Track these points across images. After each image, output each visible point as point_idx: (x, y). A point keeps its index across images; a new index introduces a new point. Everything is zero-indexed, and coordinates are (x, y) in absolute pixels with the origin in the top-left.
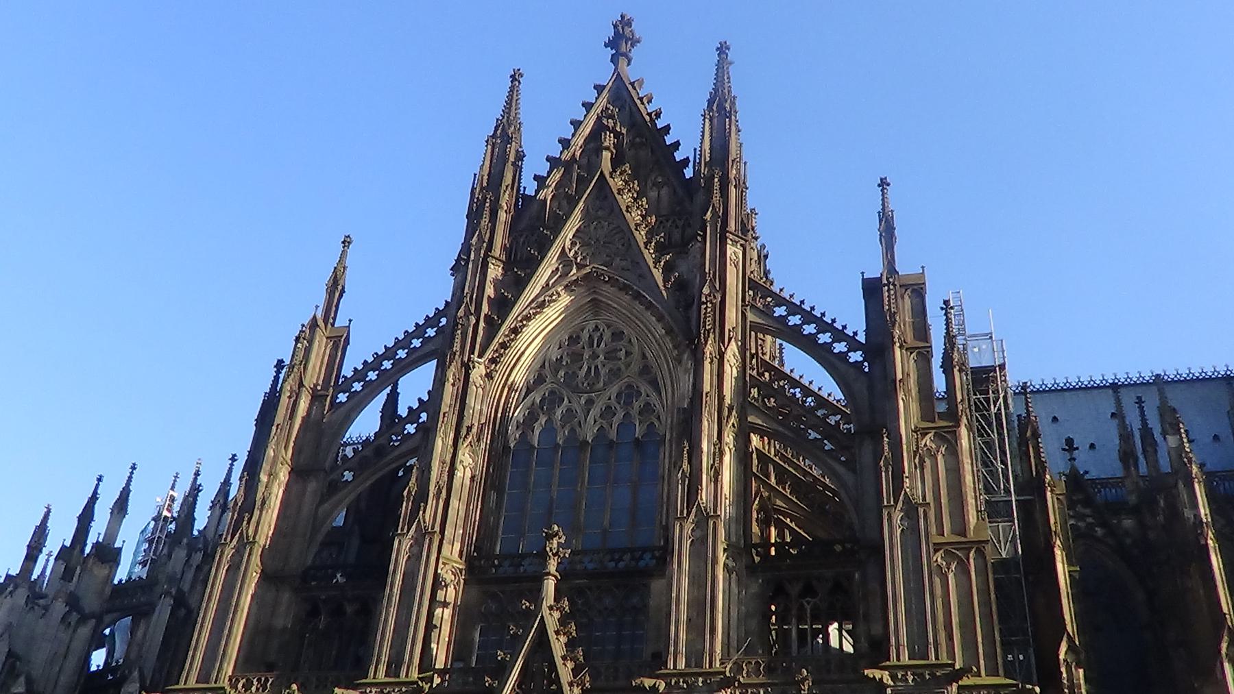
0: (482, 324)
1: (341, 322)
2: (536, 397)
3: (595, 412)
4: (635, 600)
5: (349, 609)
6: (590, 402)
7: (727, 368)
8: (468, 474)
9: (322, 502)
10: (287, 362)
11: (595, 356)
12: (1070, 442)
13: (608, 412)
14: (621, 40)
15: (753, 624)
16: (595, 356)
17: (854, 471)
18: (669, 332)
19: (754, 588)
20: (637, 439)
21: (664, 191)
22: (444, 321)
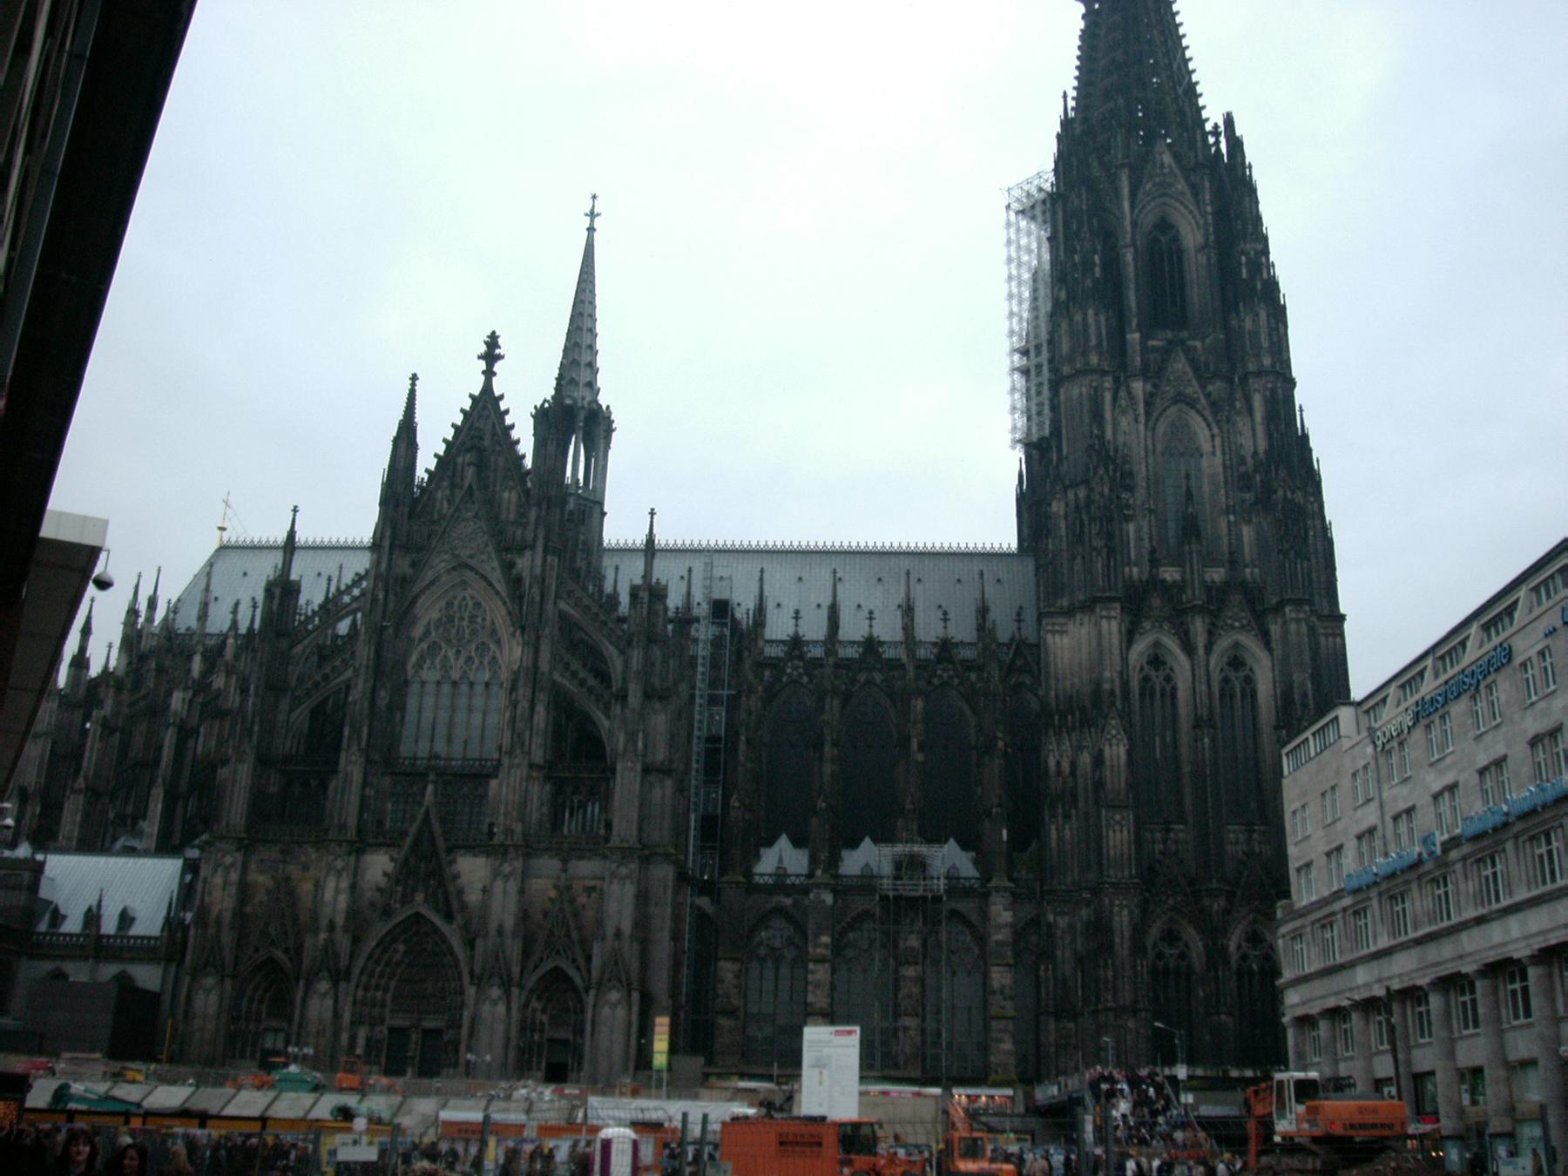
0: (391, 596)
1: (294, 576)
2: (424, 646)
4: (480, 791)
5: (313, 783)
6: (458, 652)
9: (291, 711)
10: (260, 604)
11: (462, 619)
12: (797, 612)
13: (469, 659)
14: (491, 355)
15: (545, 810)
16: (462, 619)
17: (608, 717)
18: (510, 613)
19: (548, 788)
20: (487, 685)
21: (514, 495)
22: (364, 584)
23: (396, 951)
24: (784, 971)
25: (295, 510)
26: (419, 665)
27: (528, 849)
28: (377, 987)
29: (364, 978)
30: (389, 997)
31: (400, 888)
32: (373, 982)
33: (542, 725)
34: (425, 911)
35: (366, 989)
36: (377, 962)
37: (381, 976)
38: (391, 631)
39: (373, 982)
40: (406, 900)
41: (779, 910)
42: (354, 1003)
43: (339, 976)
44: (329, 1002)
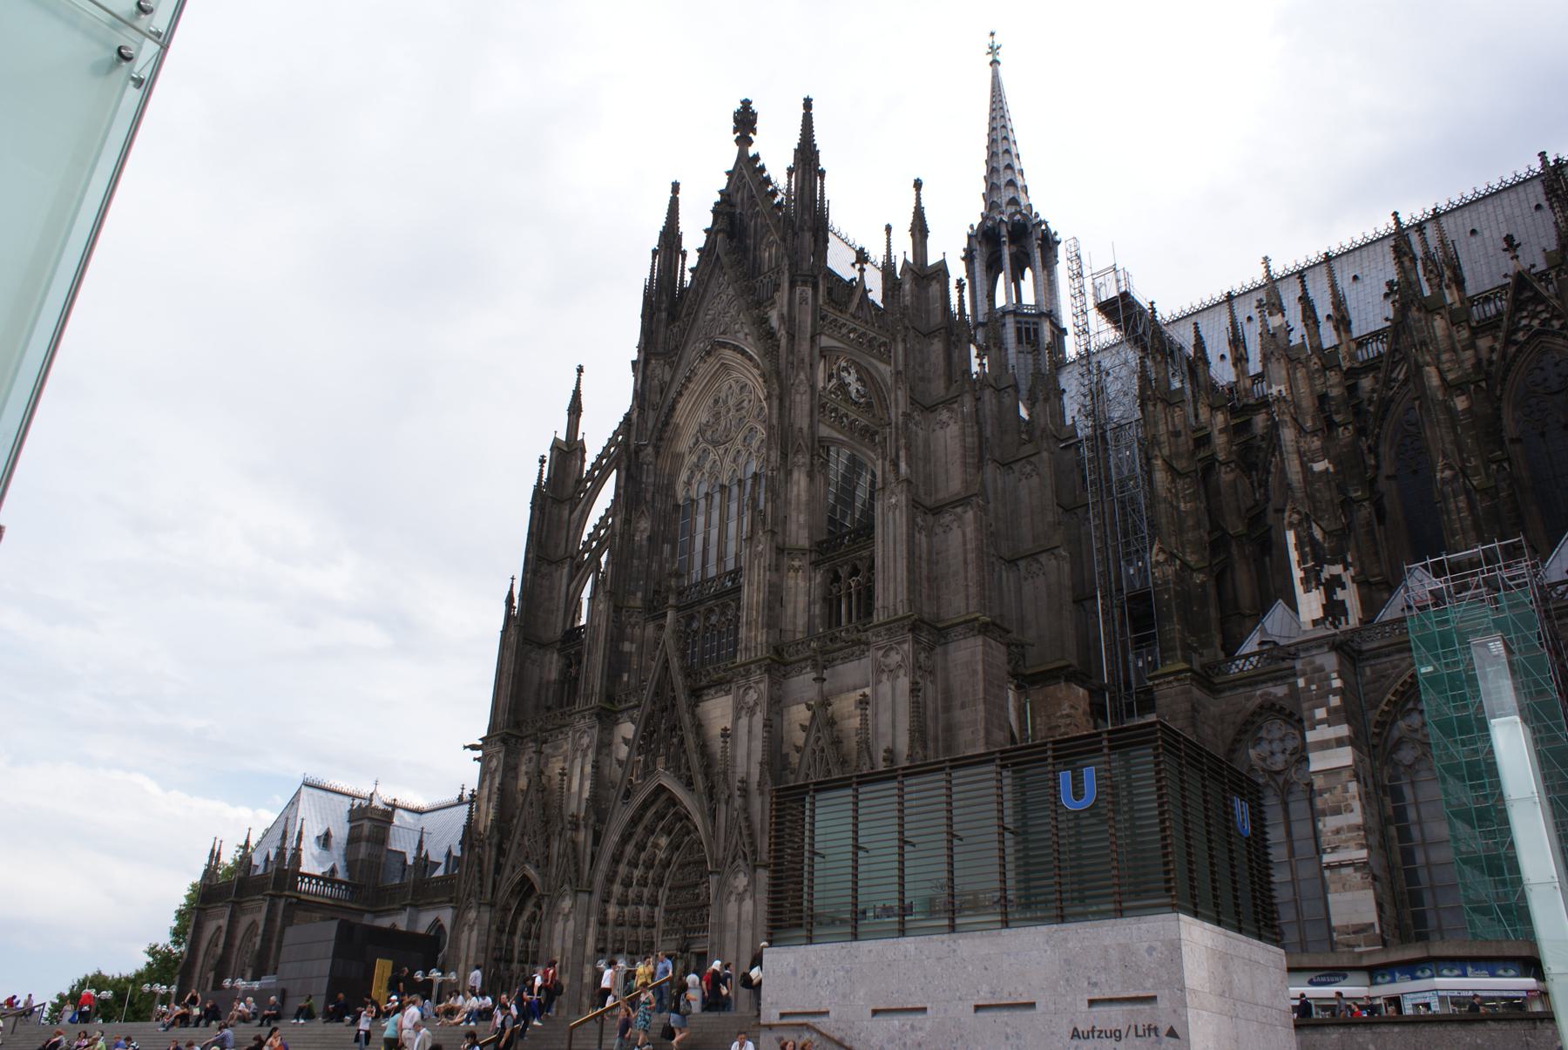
1: (580, 437)
3: (728, 460)
7: (798, 398)
8: (645, 535)
15: (817, 609)
19: (818, 579)
23: (656, 845)
24: (1298, 808)
25: (580, 370)
26: (688, 483)
27: (779, 663)
28: (639, 901)
29: (617, 889)
30: (659, 913)
31: (641, 758)
32: (631, 893)
33: (804, 497)
34: (666, 782)
35: (623, 903)
36: (633, 864)
37: (643, 882)
38: (650, 449)
39: (631, 893)
40: (648, 771)
41: (1270, 709)
42: (603, 923)
43: (581, 886)
44: (571, 924)
